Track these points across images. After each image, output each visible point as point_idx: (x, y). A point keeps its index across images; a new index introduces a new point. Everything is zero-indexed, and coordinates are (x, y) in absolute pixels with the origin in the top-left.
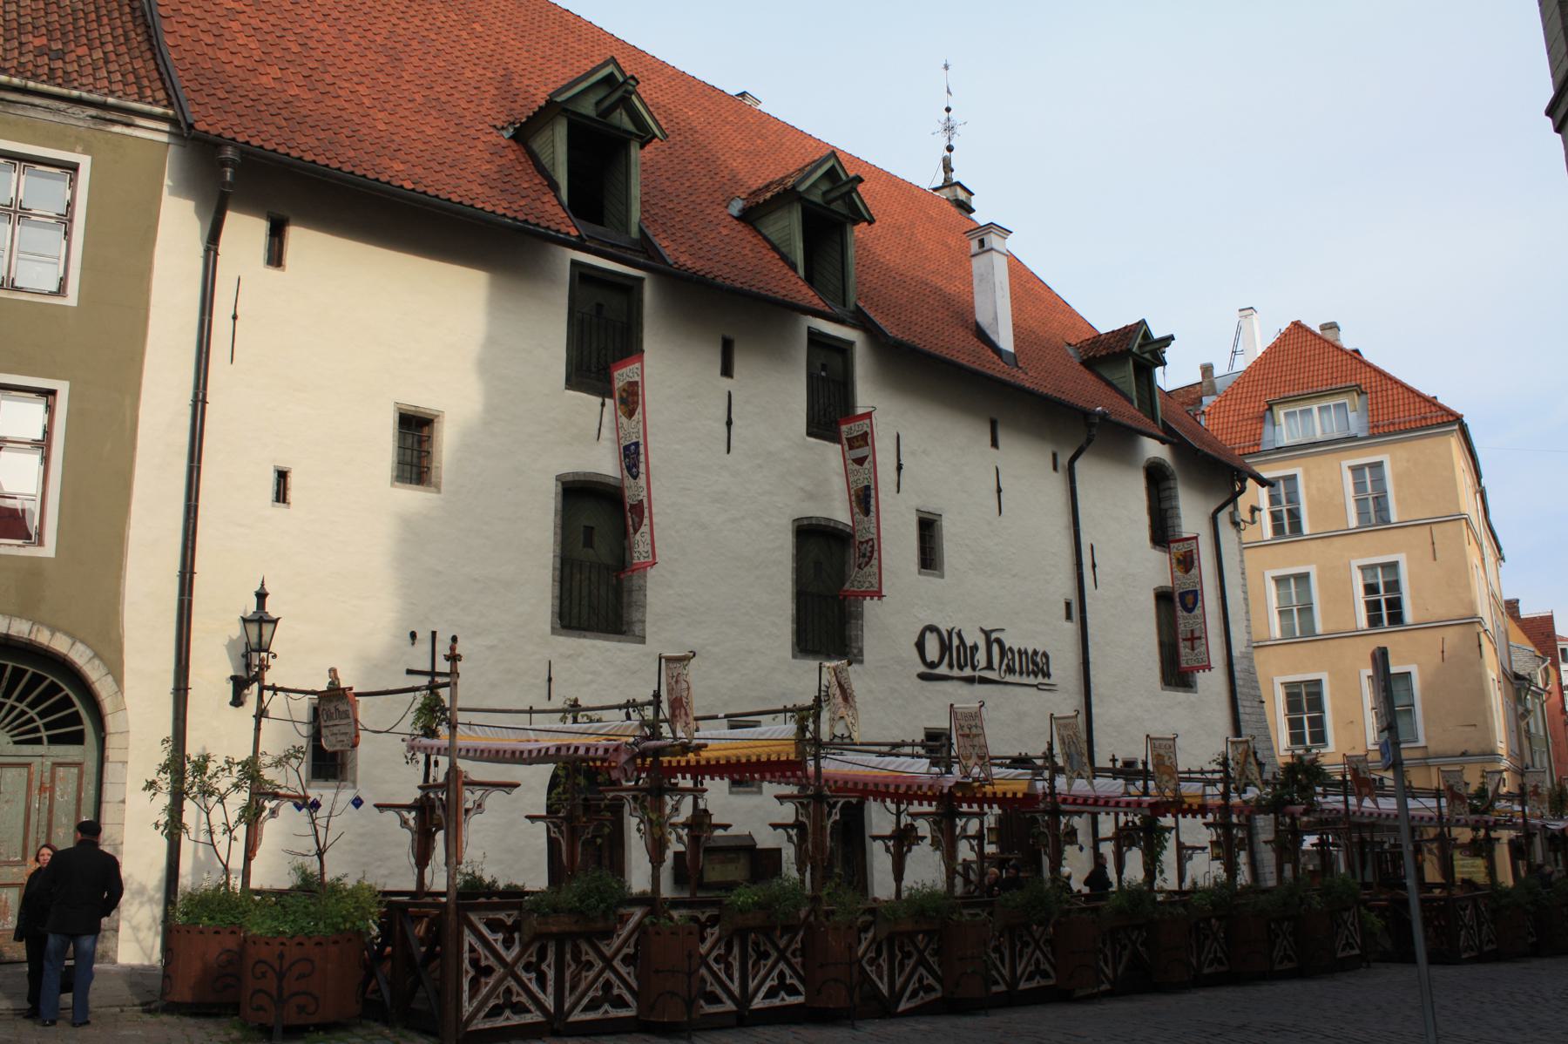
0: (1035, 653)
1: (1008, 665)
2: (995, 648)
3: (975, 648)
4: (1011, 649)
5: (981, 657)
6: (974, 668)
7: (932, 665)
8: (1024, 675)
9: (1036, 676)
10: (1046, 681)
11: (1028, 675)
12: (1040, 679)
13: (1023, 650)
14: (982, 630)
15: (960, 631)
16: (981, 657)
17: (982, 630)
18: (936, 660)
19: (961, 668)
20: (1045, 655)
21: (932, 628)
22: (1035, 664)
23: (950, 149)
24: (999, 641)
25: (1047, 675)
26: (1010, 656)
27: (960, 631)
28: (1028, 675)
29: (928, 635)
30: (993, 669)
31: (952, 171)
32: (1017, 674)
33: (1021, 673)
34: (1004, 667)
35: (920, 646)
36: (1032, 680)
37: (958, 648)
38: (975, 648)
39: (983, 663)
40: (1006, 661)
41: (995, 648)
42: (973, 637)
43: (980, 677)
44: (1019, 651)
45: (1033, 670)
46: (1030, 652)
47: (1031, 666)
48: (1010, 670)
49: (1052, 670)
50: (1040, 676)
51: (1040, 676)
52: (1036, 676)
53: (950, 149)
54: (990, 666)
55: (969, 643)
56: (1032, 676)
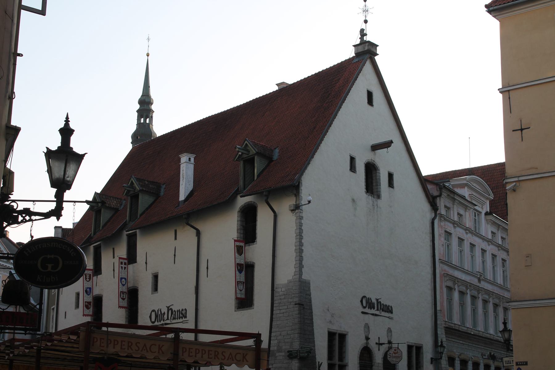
0: (182, 310)
1: (173, 317)
2: (170, 312)
3: (164, 313)
4: (175, 311)
5: (166, 316)
6: (164, 321)
7: (153, 322)
8: (179, 319)
9: (182, 318)
10: (185, 319)
11: (180, 319)
12: (184, 319)
13: (178, 310)
14: (167, 307)
15: (161, 309)
16: (166, 316)
17: (167, 307)
18: (154, 321)
19: (160, 322)
20: (186, 310)
21: (153, 311)
22: (182, 314)
23: (366, 22)
24: (171, 309)
25: (186, 317)
26: (174, 313)
27: (161, 309)
28: (180, 319)
29: (153, 313)
30: (169, 320)
31: (366, 35)
32: (176, 319)
33: (177, 319)
34: (172, 318)
35: (150, 317)
36: (181, 320)
37: (160, 315)
38: (164, 313)
39: (166, 318)
40: (173, 315)
41: (170, 312)
42: (164, 310)
43: (165, 323)
44: (177, 311)
45: (181, 316)
46: (181, 310)
47: (181, 315)
48: (174, 319)
49: (187, 315)
50: (184, 318)
51: (184, 318)
52: (182, 318)
53: (366, 22)
54: (168, 319)
55: (163, 312)
56: (181, 319)
